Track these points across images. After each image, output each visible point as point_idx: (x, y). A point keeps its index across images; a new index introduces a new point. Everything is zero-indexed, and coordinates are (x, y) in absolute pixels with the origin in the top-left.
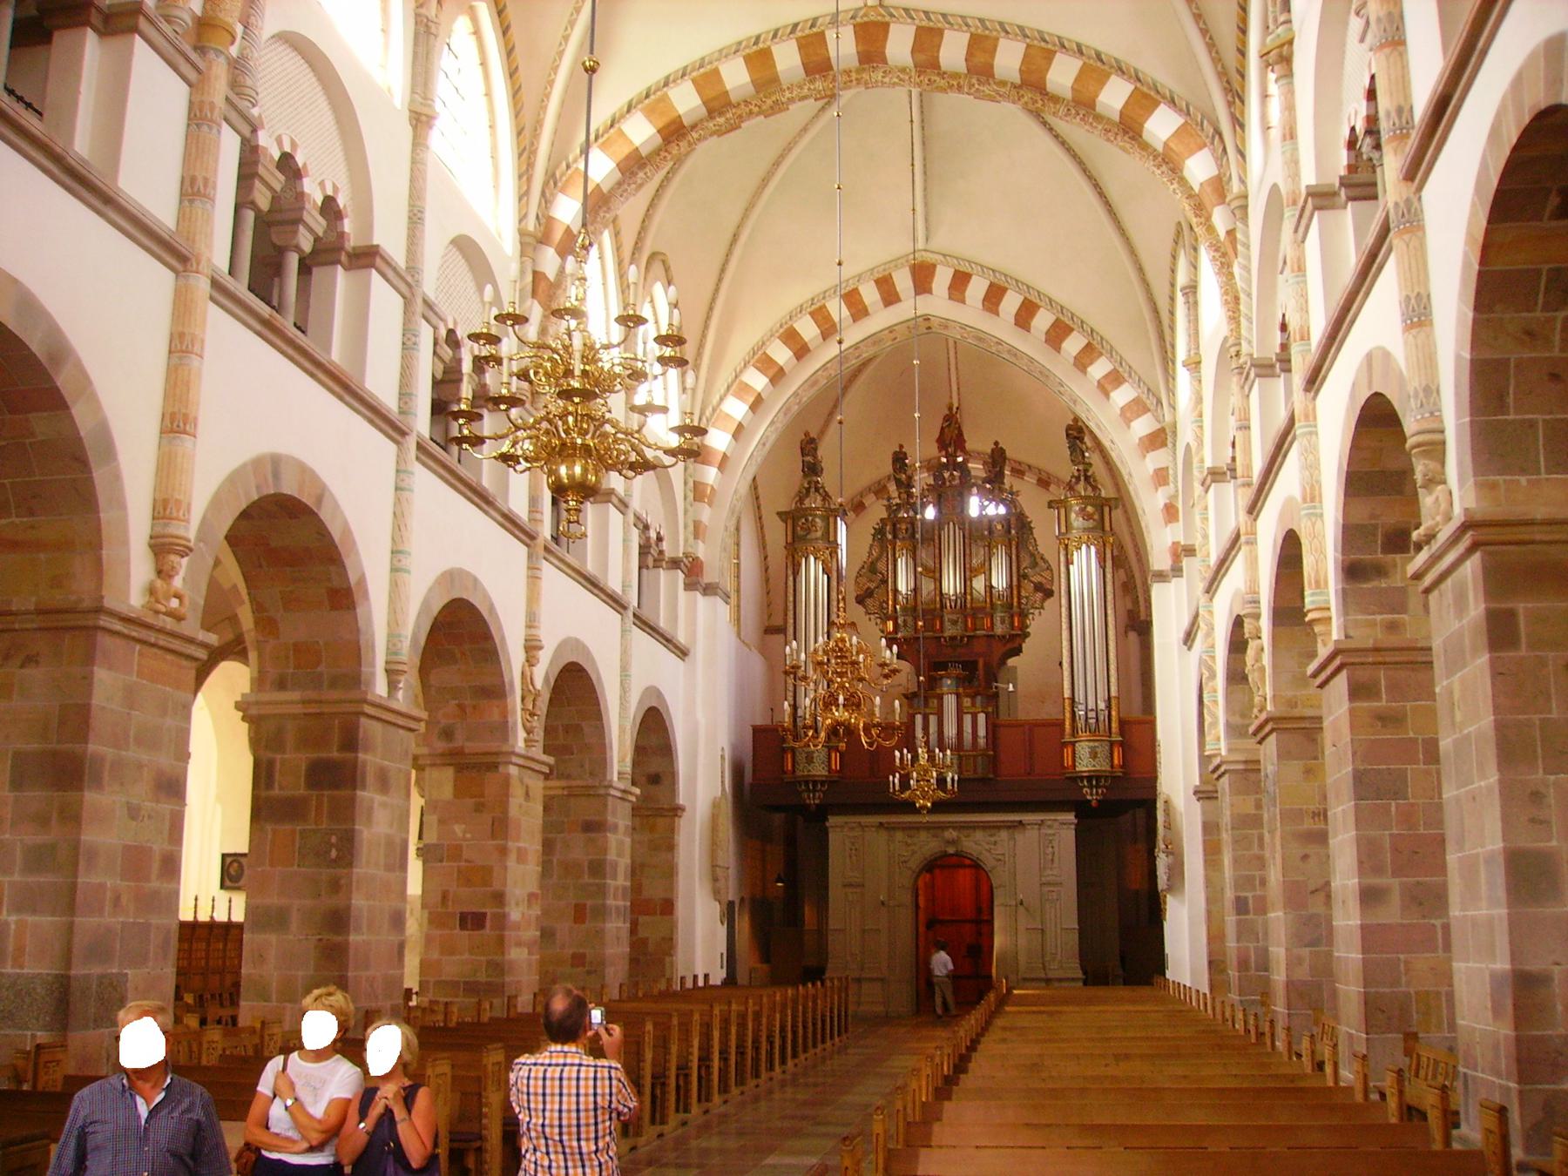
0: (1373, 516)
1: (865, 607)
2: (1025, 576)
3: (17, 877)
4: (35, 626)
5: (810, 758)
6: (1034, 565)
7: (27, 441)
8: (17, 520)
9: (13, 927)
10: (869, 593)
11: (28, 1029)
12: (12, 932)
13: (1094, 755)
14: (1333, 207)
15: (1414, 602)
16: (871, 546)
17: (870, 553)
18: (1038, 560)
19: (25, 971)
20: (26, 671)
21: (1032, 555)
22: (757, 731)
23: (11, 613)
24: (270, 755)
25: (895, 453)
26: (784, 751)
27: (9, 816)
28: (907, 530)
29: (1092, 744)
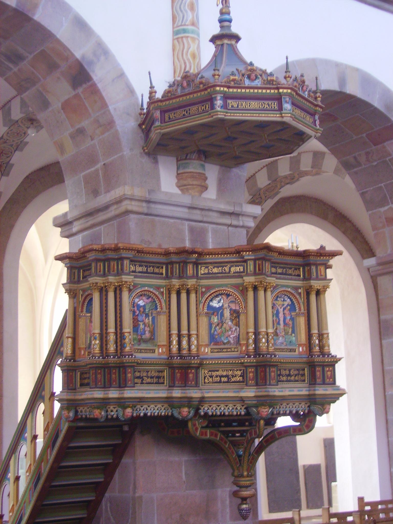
7: (387, 159)
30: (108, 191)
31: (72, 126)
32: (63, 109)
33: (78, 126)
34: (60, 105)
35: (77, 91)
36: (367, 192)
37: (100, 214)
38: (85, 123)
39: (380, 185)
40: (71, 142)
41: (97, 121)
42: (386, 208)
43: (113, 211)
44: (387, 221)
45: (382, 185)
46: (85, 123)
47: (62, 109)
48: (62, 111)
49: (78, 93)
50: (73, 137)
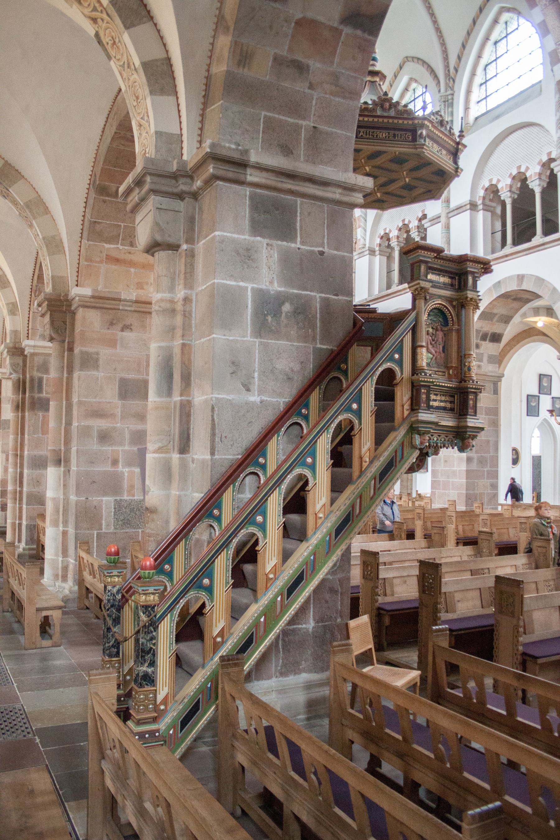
0: (482, 328)
3: (127, 448)
4: (133, 309)
8: (121, 247)
9: (126, 475)
11: (139, 528)
12: (126, 477)
14: (474, 210)
15: (485, 359)
19: (135, 498)
20: (124, 334)
23: (120, 300)
24: (40, 375)
27: (120, 414)
30: (312, 159)
31: (290, 50)
32: (299, 23)
33: (299, 57)
34: (300, 16)
35: (341, 27)
36: (99, 223)
37: (307, 184)
38: (315, 65)
39: (119, 223)
40: (270, 64)
41: (336, 77)
42: (112, 246)
43: (336, 194)
44: (106, 258)
45: (122, 224)
46: (315, 65)
47: (296, 23)
48: (293, 24)
49: (342, 31)
50: (278, 61)
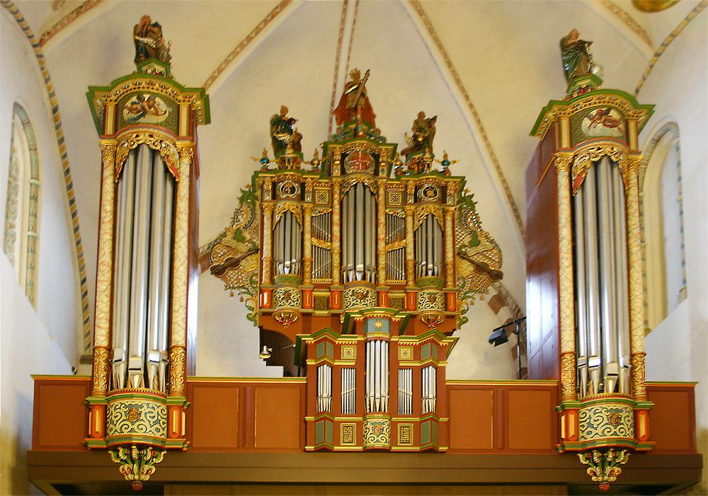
1: (224, 279)
2: (463, 256)
5: (133, 414)
6: (475, 242)
10: (234, 264)
13: (615, 419)
16: (237, 212)
17: (235, 219)
18: (483, 240)
21: (473, 234)
22: (43, 385)
25: (276, 116)
26: (89, 408)
28: (293, 190)
29: (611, 406)
